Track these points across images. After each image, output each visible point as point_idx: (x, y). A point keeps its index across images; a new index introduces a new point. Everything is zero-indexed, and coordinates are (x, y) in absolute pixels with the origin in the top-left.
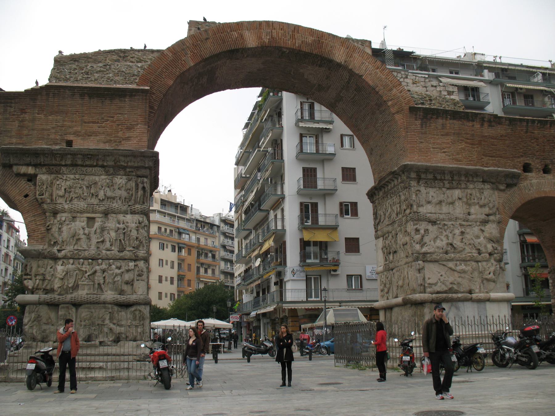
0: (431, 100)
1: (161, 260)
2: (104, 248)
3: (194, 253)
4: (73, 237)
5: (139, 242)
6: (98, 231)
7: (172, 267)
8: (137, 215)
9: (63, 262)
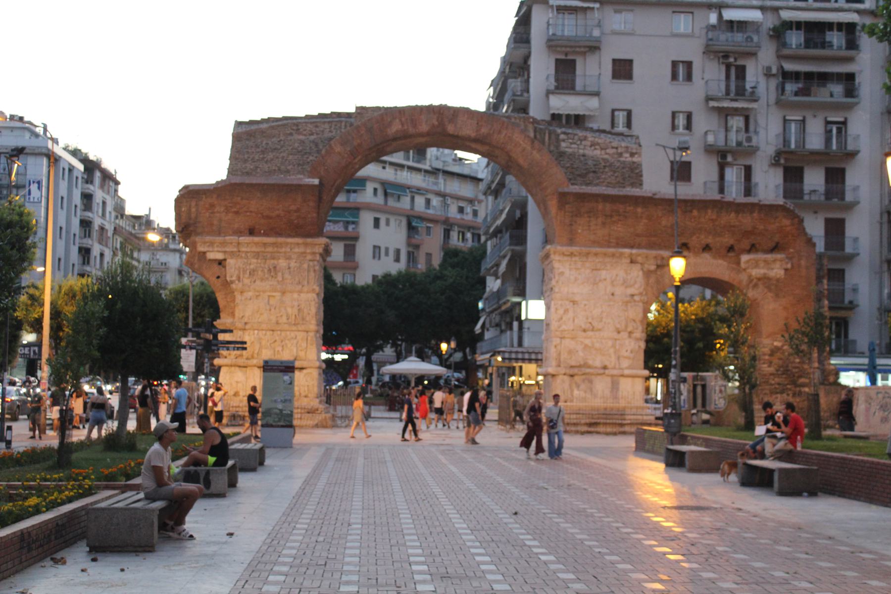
0: (605, 167)
1: (376, 248)
3: (438, 232)
4: (258, 311)
7: (397, 260)
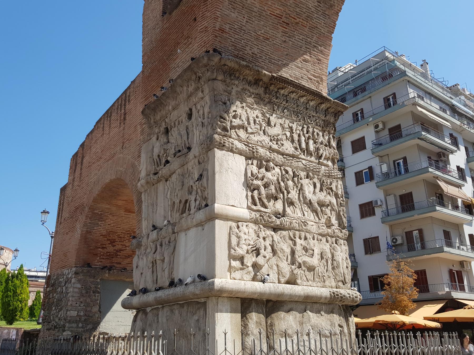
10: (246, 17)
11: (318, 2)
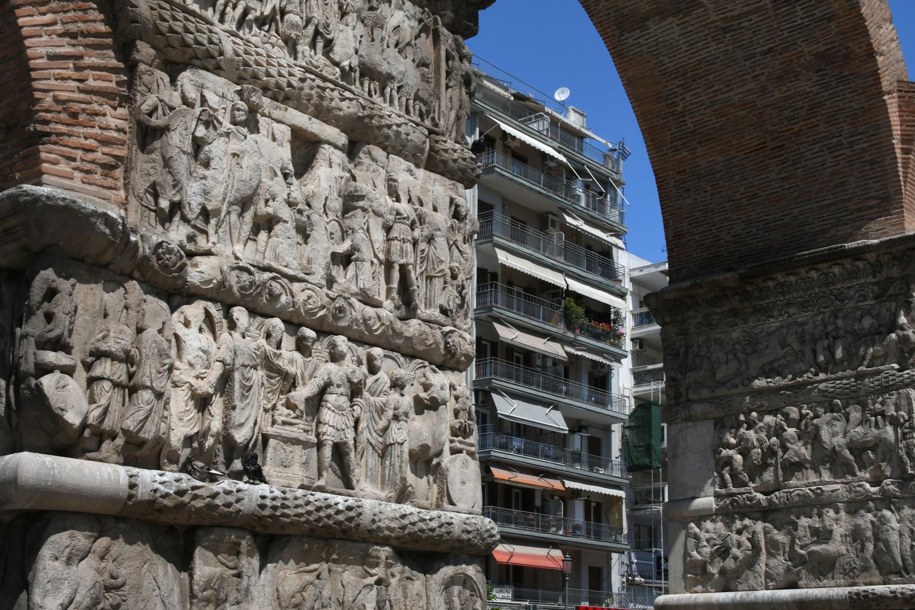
2: (354, 288)
5: (460, 293)
6: (336, 204)
8: (448, 182)
9: (208, 316)
10: (709, 189)
11: (817, 72)
